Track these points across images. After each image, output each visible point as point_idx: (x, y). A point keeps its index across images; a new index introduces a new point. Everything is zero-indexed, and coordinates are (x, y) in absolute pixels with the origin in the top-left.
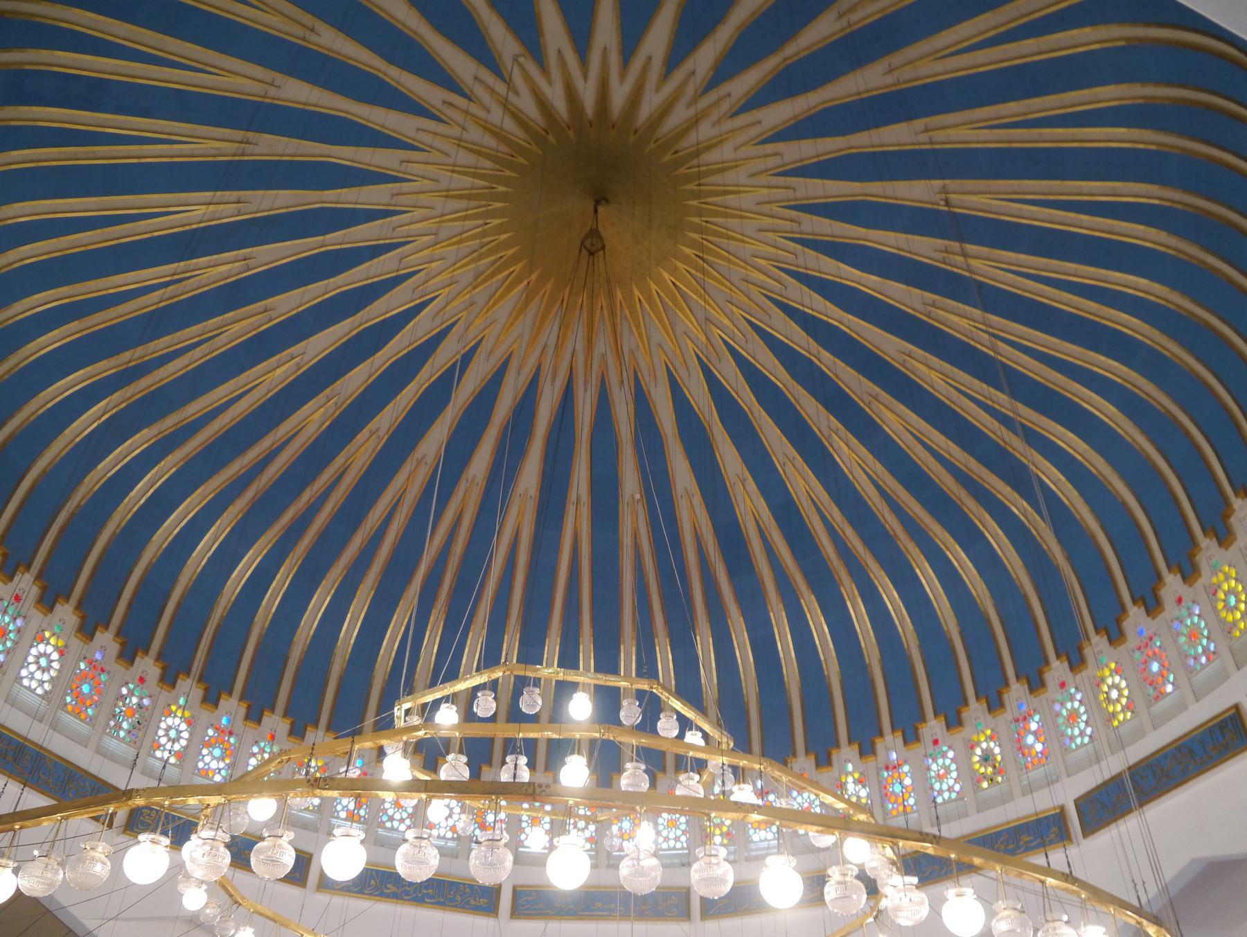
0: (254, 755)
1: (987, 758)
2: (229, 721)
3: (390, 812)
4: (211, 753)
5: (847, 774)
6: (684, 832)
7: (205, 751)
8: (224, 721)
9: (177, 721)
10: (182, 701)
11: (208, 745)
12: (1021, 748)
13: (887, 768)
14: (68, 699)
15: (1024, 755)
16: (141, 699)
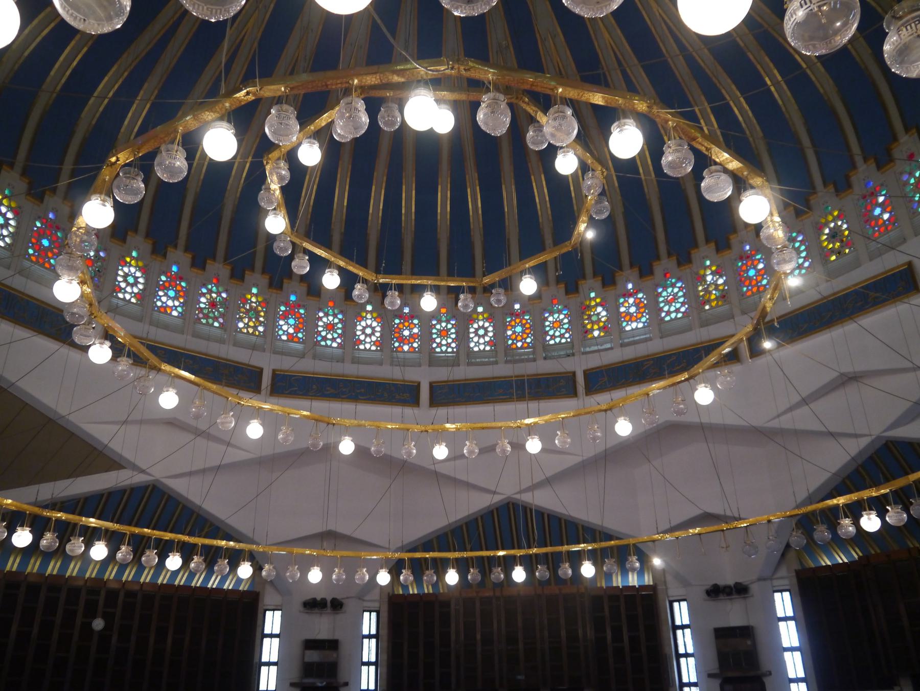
0: (204, 295)
1: (835, 235)
2: (179, 269)
3: (324, 334)
4: (166, 295)
5: (706, 268)
6: (567, 330)
7: (161, 293)
8: (174, 269)
9: (133, 270)
10: (134, 254)
11: (164, 288)
12: (868, 218)
13: (741, 258)
14: (31, 251)
15: (870, 225)
16: (97, 251)
